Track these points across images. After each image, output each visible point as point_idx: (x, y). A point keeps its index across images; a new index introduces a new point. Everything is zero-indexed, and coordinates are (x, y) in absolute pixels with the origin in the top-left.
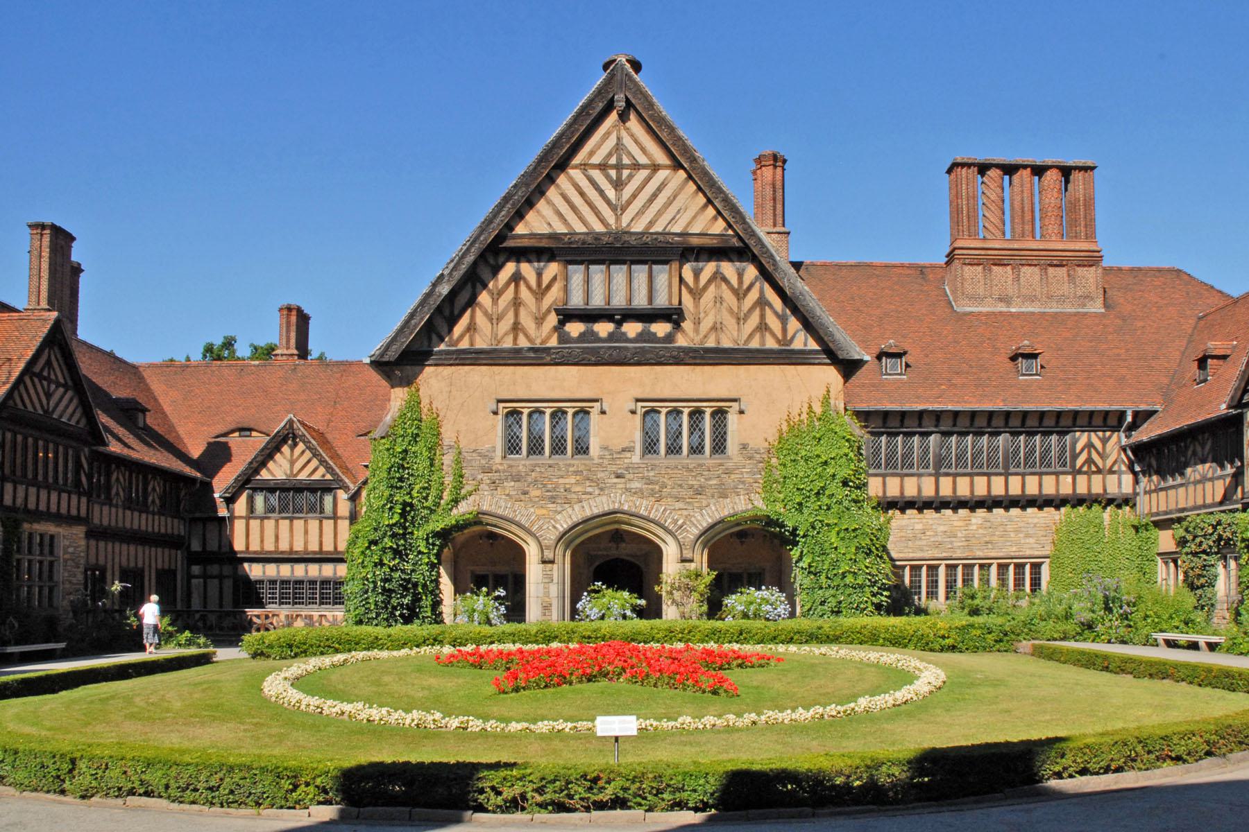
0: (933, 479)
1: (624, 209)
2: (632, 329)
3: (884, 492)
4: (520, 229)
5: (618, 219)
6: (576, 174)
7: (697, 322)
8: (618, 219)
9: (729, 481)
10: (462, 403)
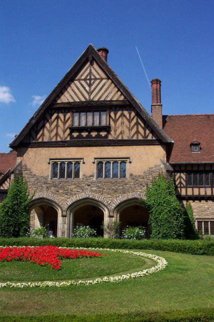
0: (210, 189)
1: (91, 93)
2: (94, 134)
3: (193, 193)
4: (59, 101)
5: (90, 97)
6: (76, 82)
7: (115, 131)
8: (90, 97)
9: (127, 187)
10: (38, 162)
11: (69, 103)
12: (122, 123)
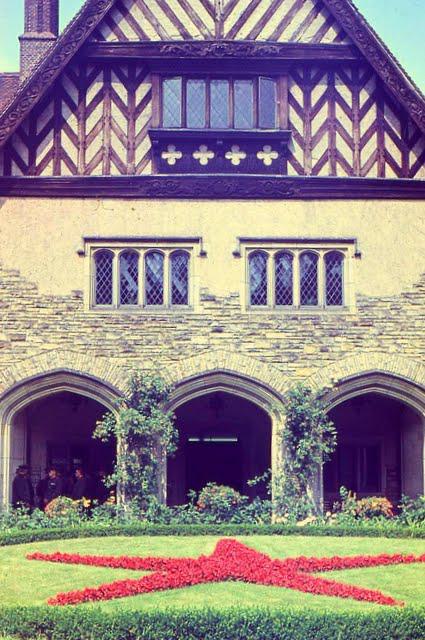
1: (224, 17)
8: (220, 24)
11: (145, 45)
12: (332, 125)
